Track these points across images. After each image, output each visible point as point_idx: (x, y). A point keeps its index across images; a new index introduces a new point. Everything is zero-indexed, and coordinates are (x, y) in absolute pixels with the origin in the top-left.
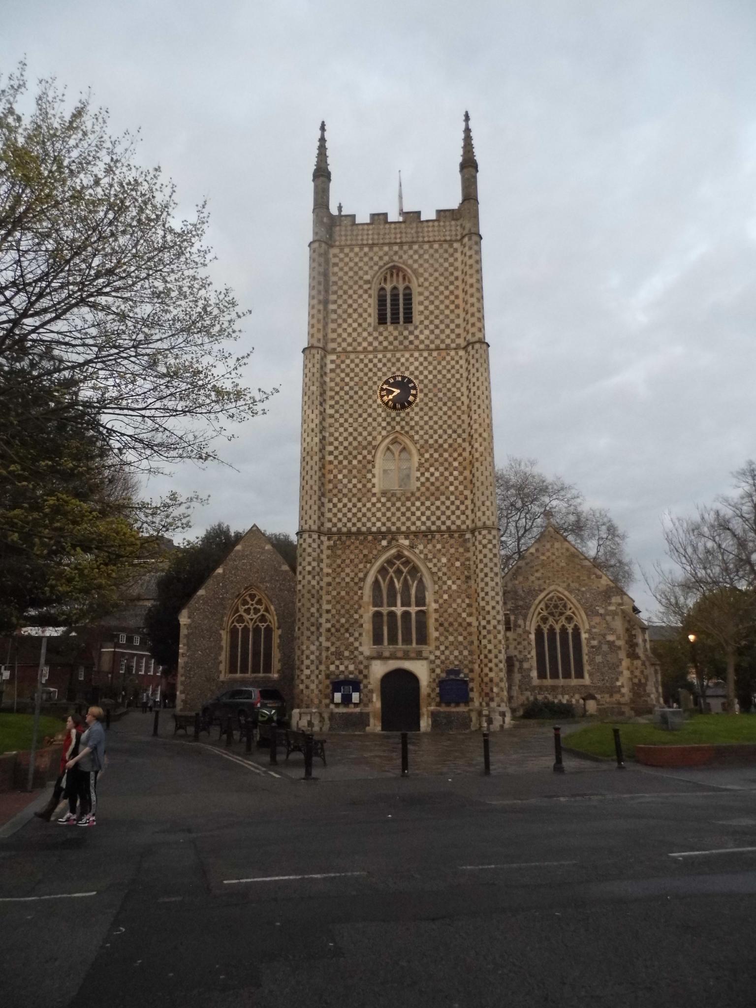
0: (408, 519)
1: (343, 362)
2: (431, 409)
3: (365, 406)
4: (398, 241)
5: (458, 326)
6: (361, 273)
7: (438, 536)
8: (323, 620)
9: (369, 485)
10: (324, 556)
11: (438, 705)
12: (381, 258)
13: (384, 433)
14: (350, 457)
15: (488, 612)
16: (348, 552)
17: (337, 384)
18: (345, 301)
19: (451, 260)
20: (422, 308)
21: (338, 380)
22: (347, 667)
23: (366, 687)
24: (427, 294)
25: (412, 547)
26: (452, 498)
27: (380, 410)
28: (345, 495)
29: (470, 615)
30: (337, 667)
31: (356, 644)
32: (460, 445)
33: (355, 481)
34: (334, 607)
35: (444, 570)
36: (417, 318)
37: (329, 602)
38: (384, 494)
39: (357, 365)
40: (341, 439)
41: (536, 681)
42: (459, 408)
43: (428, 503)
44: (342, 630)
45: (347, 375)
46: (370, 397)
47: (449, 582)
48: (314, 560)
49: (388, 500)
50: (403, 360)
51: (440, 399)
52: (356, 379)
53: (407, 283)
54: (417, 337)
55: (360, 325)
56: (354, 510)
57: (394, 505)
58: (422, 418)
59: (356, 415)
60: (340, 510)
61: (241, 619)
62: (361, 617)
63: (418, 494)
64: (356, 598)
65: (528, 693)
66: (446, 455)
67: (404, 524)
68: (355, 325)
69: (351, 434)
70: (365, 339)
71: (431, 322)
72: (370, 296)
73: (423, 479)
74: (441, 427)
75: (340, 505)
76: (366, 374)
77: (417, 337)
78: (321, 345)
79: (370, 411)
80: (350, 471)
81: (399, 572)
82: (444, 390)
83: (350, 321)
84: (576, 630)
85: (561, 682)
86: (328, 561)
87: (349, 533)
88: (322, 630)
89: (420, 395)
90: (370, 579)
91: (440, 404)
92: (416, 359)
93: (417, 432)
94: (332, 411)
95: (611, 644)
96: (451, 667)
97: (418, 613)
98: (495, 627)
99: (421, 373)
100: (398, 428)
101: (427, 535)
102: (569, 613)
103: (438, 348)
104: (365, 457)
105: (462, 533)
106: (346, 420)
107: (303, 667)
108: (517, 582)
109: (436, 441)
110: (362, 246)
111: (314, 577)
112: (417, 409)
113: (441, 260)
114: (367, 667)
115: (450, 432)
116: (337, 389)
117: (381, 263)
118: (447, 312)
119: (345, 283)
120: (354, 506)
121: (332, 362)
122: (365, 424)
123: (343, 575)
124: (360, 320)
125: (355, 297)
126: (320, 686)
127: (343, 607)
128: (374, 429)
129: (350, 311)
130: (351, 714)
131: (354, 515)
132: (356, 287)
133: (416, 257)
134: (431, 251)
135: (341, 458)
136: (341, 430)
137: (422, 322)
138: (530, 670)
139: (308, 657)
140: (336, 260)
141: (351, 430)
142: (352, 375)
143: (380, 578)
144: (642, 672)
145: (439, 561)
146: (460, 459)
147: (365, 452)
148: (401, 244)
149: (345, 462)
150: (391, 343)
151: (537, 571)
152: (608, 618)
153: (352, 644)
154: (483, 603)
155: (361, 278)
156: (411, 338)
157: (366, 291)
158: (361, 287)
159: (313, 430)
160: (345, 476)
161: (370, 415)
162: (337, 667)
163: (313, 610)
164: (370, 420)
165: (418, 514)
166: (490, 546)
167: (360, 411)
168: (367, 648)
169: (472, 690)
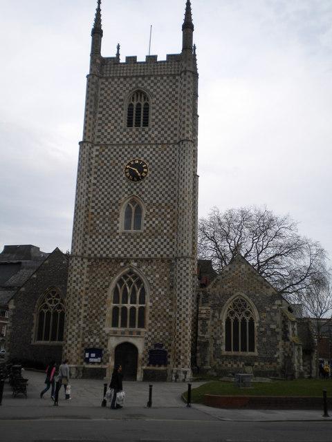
0: (138, 250)
1: (103, 151)
2: (155, 181)
3: (116, 179)
4: (142, 74)
5: (175, 129)
6: (118, 94)
7: (154, 261)
8: (82, 311)
9: (115, 228)
10: (85, 271)
11: (148, 365)
12: (130, 85)
13: (126, 196)
14: (105, 211)
15: (181, 309)
16: (99, 269)
17: (99, 165)
18: (107, 112)
19: (174, 87)
20: (154, 117)
21: (100, 162)
22: (95, 340)
23: (105, 352)
24: (158, 108)
25: (139, 267)
26: (165, 237)
27: (124, 181)
28: (100, 234)
29: (171, 310)
30: (89, 340)
31: (101, 326)
32: (172, 204)
33: (106, 225)
34: (89, 303)
35: (157, 282)
36: (151, 123)
37: (86, 300)
38: (124, 234)
39: (112, 153)
40: (100, 199)
41: (224, 353)
42: (173, 181)
43: (150, 240)
44: (94, 317)
45: (106, 159)
46: (119, 173)
47: (160, 290)
48: (78, 274)
49: (126, 238)
50: (140, 150)
51: (162, 175)
52: (111, 161)
53: (146, 101)
54: (150, 136)
55: (115, 127)
56: (105, 243)
57: (129, 240)
58: (150, 187)
59: (109, 184)
60: (96, 243)
61: (46, 307)
62: (105, 309)
63: (144, 234)
64: (103, 297)
65: (218, 360)
66: (163, 210)
67: (134, 252)
68: (112, 127)
69: (106, 196)
70: (118, 136)
71: (159, 126)
72: (123, 109)
73: (148, 225)
74: (161, 193)
75: (97, 240)
76: (117, 159)
77: (150, 136)
78: (91, 141)
79: (118, 181)
80: (104, 219)
81: (130, 283)
82: (165, 169)
83: (109, 125)
84: (252, 321)
85: (240, 353)
86: (87, 275)
87: (101, 259)
88: (81, 317)
89: (150, 172)
90: (112, 288)
91: (161, 178)
92: (148, 150)
93: (146, 196)
94: (95, 181)
95: (273, 330)
96: (158, 342)
97: (140, 308)
98: (184, 319)
99: (151, 158)
100: (135, 193)
101: (149, 261)
102: (248, 310)
103: (162, 143)
104: (113, 211)
105: (169, 261)
106: (103, 187)
107: (68, 339)
108: (216, 289)
109: (157, 201)
110: (119, 78)
111: (77, 284)
112: (147, 181)
113: (168, 87)
114: (107, 340)
115: (166, 196)
116: (99, 167)
117: (130, 88)
118: (169, 120)
119: (108, 101)
120: (105, 240)
121: (97, 150)
122: (115, 190)
123: (96, 283)
124: (116, 124)
125: (114, 109)
126: (78, 351)
127: (95, 303)
128: (120, 193)
129: (110, 118)
130: (95, 369)
131: (105, 246)
132: (114, 103)
133: (152, 85)
134: (162, 81)
135: (99, 210)
136: (100, 193)
137: (153, 126)
139: (70, 333)
140: (103, 86)
141: (106, 193)
142: (108, 159)
143: (118, 286)
144: (290, 350)
145: (155, 276)
146: (172, 213)
147: (114, 207)
148: (143, 77)
149: (101, 213)
150: (134, 139)
152: (272, 314)
153: (99, 326)
154: (178, 304)
155: (118, 98)
156: (146, 136)
157: (120, 106)
158: (117, 103)
159: (82, 194)
160: (101, 222)
161: (118, 184)
162: (89, 340)
163: (76, 304)
164: (118, 187)
165: (144, 246)
166: (185, 268)
167: (112, 182)
168: (108, 329)
169: (169, 357)
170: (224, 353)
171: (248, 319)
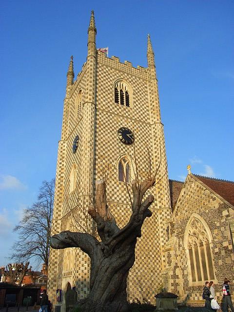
170: (191, 284)
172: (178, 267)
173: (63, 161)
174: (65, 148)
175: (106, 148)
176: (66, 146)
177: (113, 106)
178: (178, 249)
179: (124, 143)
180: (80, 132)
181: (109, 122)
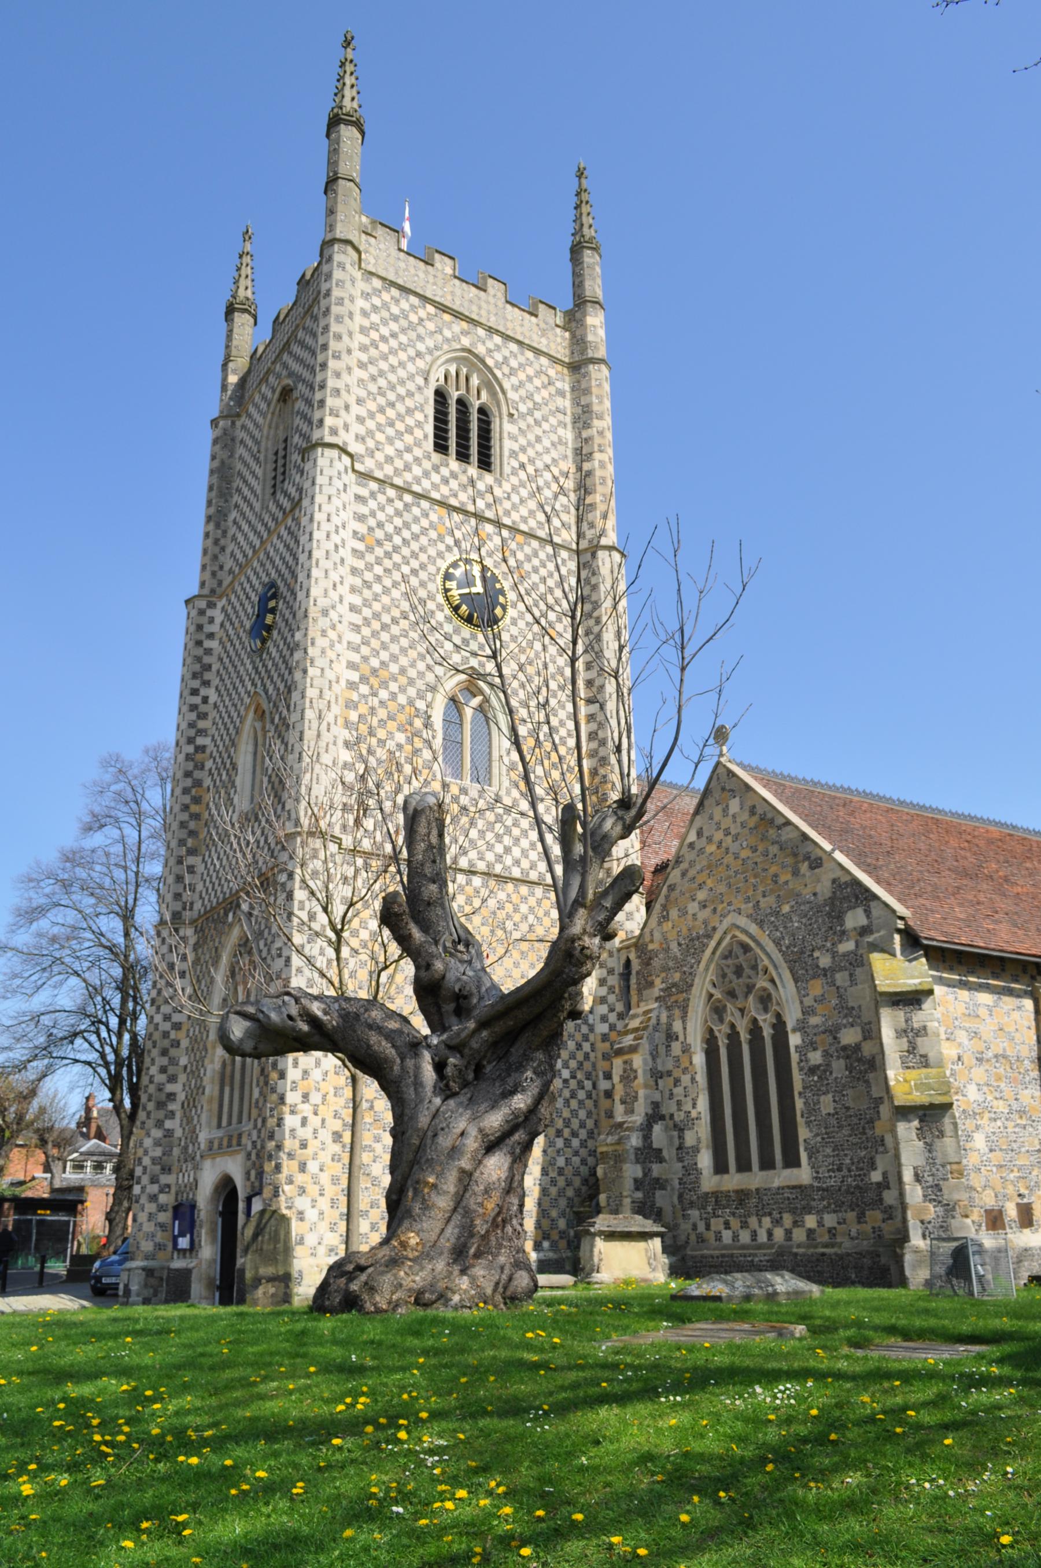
84: (779, 1026)
85: (756, 1179)
102: (762, 983)
138: (696, 1150)
151: (700, 886)
170: (709, 1181)
171: (766, 1022)
172: (662, 1118)
173: (206, 683)
174: (215, 628)
175: (394, 639)
176: (218, 620)
177: (427, 465)
178: (662, 1050)
179: (469, 620)
180: (283, 569)
181: (406, 534)
